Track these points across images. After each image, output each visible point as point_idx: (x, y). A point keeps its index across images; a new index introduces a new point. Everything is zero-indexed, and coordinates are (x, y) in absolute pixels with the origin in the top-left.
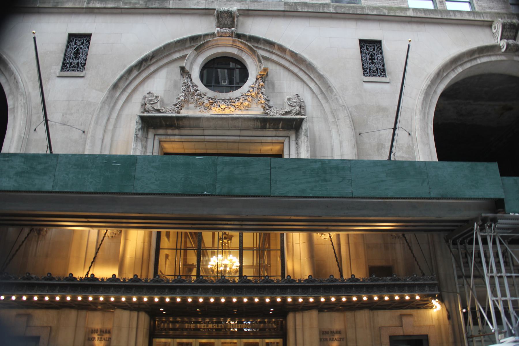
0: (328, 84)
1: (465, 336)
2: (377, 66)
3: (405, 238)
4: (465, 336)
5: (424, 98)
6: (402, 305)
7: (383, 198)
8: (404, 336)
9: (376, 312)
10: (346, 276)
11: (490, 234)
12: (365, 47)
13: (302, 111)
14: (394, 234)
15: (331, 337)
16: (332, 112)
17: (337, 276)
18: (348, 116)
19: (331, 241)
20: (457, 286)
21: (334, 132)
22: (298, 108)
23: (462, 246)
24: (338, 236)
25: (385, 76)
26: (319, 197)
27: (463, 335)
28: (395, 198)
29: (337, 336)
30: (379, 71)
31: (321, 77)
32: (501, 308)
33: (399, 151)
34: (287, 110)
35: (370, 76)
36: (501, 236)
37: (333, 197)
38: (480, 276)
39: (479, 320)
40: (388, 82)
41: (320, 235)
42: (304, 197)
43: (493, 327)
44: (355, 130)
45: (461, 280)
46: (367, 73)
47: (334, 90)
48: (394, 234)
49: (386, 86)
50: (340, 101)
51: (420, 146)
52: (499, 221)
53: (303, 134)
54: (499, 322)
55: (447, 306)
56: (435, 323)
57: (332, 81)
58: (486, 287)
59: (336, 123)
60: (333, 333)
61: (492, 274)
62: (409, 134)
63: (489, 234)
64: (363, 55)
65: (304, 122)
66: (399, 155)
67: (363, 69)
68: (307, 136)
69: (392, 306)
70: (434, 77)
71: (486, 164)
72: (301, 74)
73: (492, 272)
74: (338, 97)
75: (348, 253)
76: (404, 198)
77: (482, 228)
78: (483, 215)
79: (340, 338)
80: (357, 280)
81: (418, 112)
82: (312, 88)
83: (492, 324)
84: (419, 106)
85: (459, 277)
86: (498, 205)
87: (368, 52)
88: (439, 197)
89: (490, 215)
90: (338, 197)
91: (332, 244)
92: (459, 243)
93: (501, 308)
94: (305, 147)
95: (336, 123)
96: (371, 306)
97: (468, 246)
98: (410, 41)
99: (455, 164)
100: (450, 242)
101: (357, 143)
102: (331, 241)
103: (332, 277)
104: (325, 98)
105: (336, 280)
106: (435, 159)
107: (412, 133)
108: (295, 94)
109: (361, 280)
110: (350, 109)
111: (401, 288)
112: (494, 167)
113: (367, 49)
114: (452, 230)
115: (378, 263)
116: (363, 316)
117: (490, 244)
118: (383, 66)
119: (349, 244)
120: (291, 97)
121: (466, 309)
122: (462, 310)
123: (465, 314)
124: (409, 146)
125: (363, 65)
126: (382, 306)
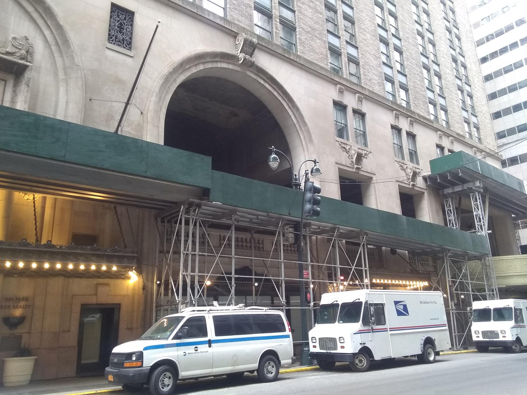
0: (66, 37)
1: (154, 305)
2: (124, 36)
3: (116, 210)
4: (154, 305)
5: (163, 82)
6: (98, 274)
7: (98, 168)
8: (97, 304)
9: (71, 280)
10: (44, 242)
11: (193, 217)
12: (116, 14)
13: (29, 57)
14: (106, 205)
15: (16, 304)
16: (65, 69)
17: (32, 240)
18: (82, 78)
19: (34, 202)
20: (157, 260)
21: (62, 90)
22: (24, 52)
23: (169, 224)
24: (44, 199)
25: (130, 49)
26: (25, 154)
27: (153, 303)
28: (111, 170)
29: (22, 304)
30: (125, 42)
31: (59, 27)
32: (188, 281)
33: (128, 126)
34: (9, 49)
35: (114, 44)
36: (203, 221)
37: (42, 157)
38: (177, 252)
39: (170, 291)
40: (132, 57)
41: (23, 195)
42: (7, 151)
43: (178, 298)
44: (86, 93)
45: (162, 255)
46: (113, 41)
47: (72, 46)
48: (106, 205)
49: (129, 60)
50: (76, 59)
51: (150, 127)
52: (203, 207)
53: (24, 82)
54: (185, 293)
55: (144, 278)
56: (130, 293)
57: (72, 36)
58: (180, 262)
59: (66, 81)
60: (18, 300)
61: (188, 252)
62: (142, 113)
63: (192, 217)
64: (112, 21)
65: (28, 69)
66: (127, 131)
67: (109, 35)
68: (28, 86)
69: (87, 275)
70: (177, 66)
71: (202, 156)
72: (35, 15)
73: (188, 251)
74: (74, 55)
75: (52, 218)
76: (120, 172)
77: (187, 212)
78: (191, 200)
79: (26, 306)
80: (54, 246)
81: (154, 94)
82: (47, 36)
83: (178, 295)
84: (157, 90)
85: (161, 252)
86: (205, 193)
87: (118, 19)
88: (154, 177)
89: (197, 201)
90: (48, 158)
91: (34, 206)
92: (166, 222)
93: (188, 281)
94: (24, 97)
95: (66, 81)
96: (64, 273)
97: (173, 225)
98: (159, 22)
99: (175, 150)
100: (159, 219)
101: (85, 108)
102: (34, 202)
103: (24, 241)
104: (60, 51)
105: (29, 245)
106: (162, 142)
107: (145, 113)
108: (23, 35)
109: (58, 247)
110: (85, 71)
111: (100, 257)
112: (208, 160)
113: (118, 16)
114: (162, 209)
115: (83, 231)
116: (57, 283)
117: (191, 227)
118: (131, 38)
119: (55, 208)
120: (17, 37)
121: (161, 281)
122: (156, 281)
123: (159, 286)
124: (139, 125)
125: (110, 30)
126: (76, 274)
